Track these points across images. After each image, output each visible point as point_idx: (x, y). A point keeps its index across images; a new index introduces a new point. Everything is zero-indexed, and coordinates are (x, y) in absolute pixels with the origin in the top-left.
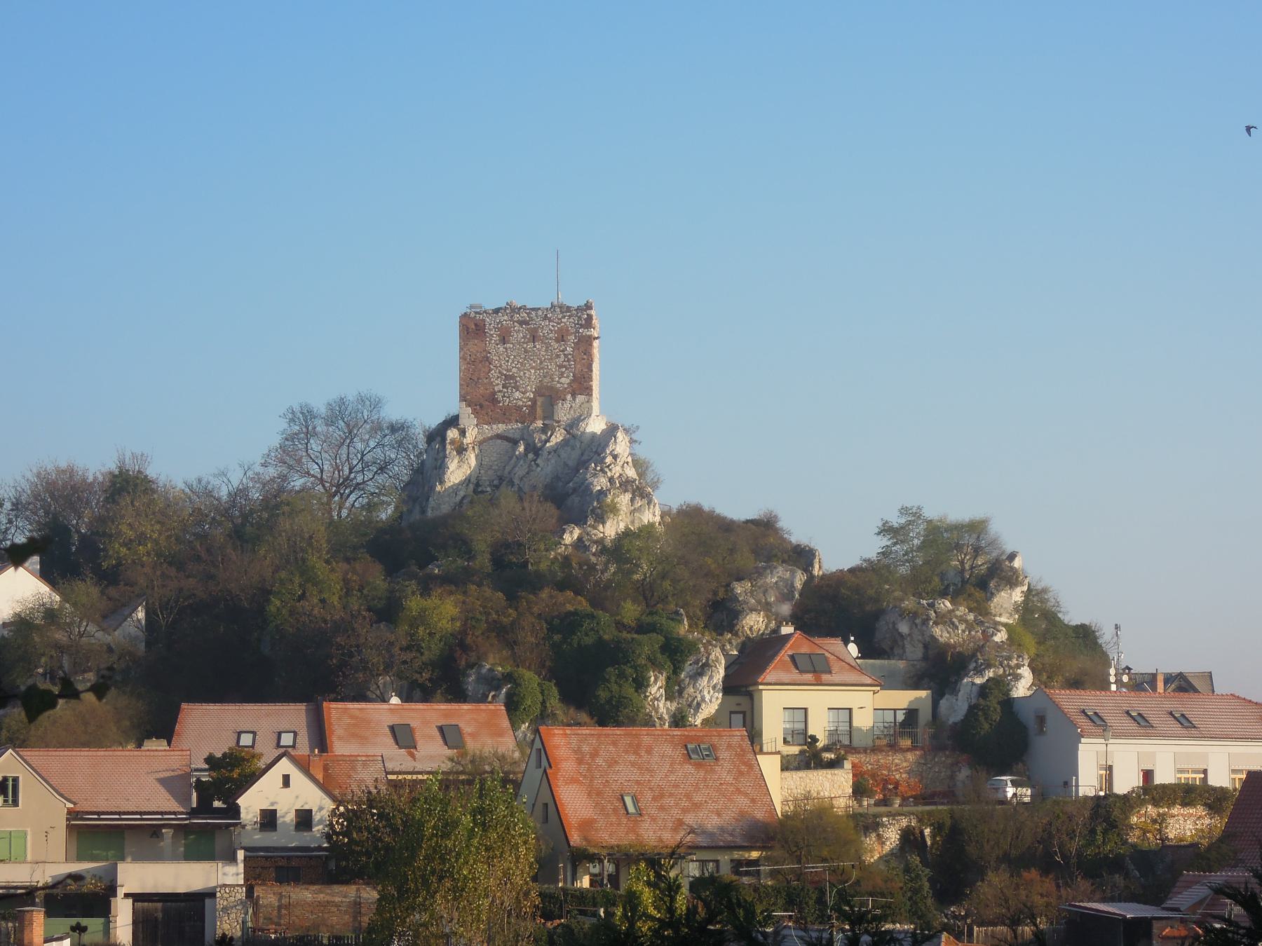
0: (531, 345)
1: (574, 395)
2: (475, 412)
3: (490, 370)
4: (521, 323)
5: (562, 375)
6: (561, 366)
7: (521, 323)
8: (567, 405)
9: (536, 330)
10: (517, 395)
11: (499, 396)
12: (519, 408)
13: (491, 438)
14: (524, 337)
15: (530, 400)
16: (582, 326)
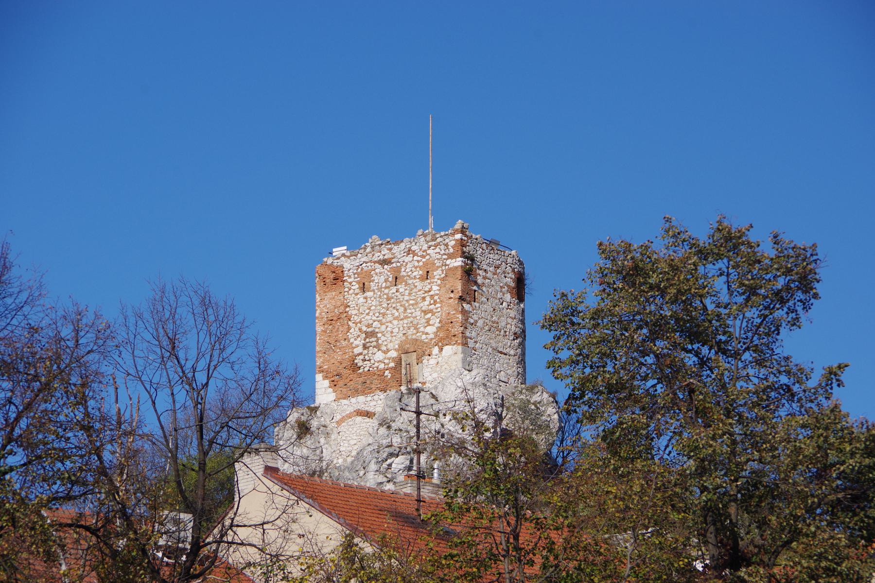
0: (394, 289)
1: (441, 350)
2: (334, 385)
3: (349, 328)
4: (384, 262)
5: (428, 323)
6: (425, 312)
7: (384, 262)
8: (433, 361)
9: (398, 270)
10: (379, 356)
11: (359, 361)
12: (381, 374)
13: (349, 416)
14: (386, 281)
15: (393, 359)
16: (451, 256)
